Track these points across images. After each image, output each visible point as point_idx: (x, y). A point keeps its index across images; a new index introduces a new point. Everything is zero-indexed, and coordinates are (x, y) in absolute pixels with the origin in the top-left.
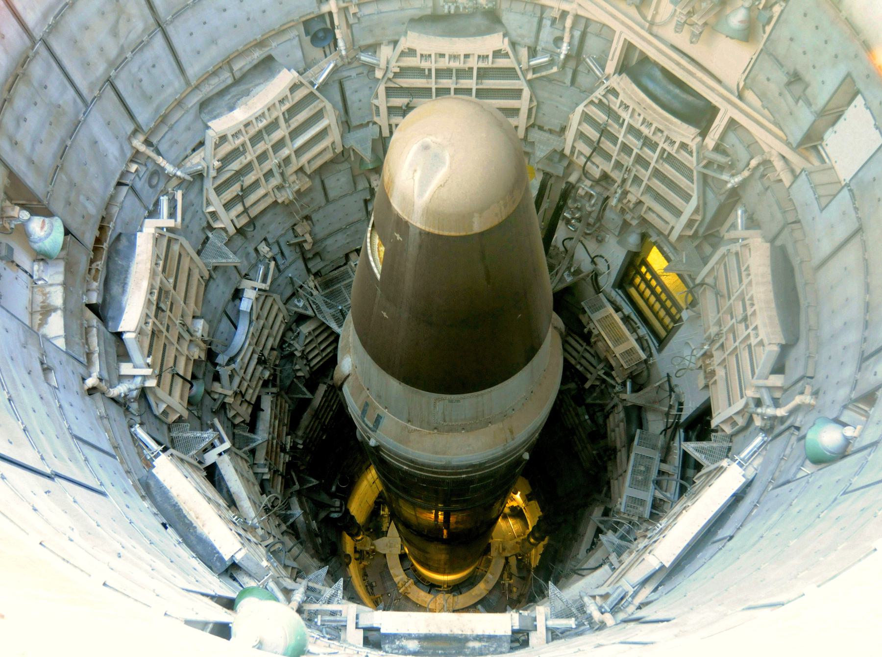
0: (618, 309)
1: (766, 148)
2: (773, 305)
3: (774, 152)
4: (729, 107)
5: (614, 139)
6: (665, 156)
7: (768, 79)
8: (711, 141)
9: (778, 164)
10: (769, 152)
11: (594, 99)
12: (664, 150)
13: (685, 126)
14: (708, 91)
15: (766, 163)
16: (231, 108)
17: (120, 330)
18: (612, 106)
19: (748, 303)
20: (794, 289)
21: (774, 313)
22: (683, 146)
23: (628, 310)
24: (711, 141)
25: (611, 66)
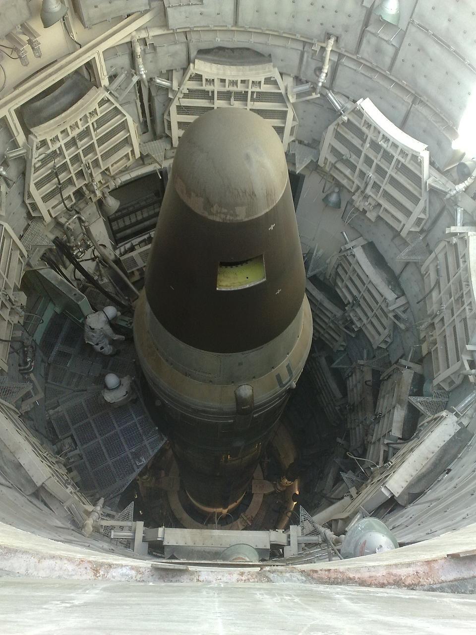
0: (132, 249)
1: (128, 40)
2: (241, 67)
3: (134, 34)
4: (97, 49)
5: (64, 167)
6: (96, 126)
7: (96, 7)
8: (105, 82)
9: (143, 35)
10: (132, 37)
11: (37, 166)
12: (92, 123)
13: (86, 97)
14: (78, 61)
15: (144, 41)
16: (19, 466)
17: (268, 547)
18: (49, 152)
19: (232, 89)
20: (233, 50)
21: (247, 68)
22: (102, 102)
23: (136, 241)
24: (105, 82)
25: (21, 138)
